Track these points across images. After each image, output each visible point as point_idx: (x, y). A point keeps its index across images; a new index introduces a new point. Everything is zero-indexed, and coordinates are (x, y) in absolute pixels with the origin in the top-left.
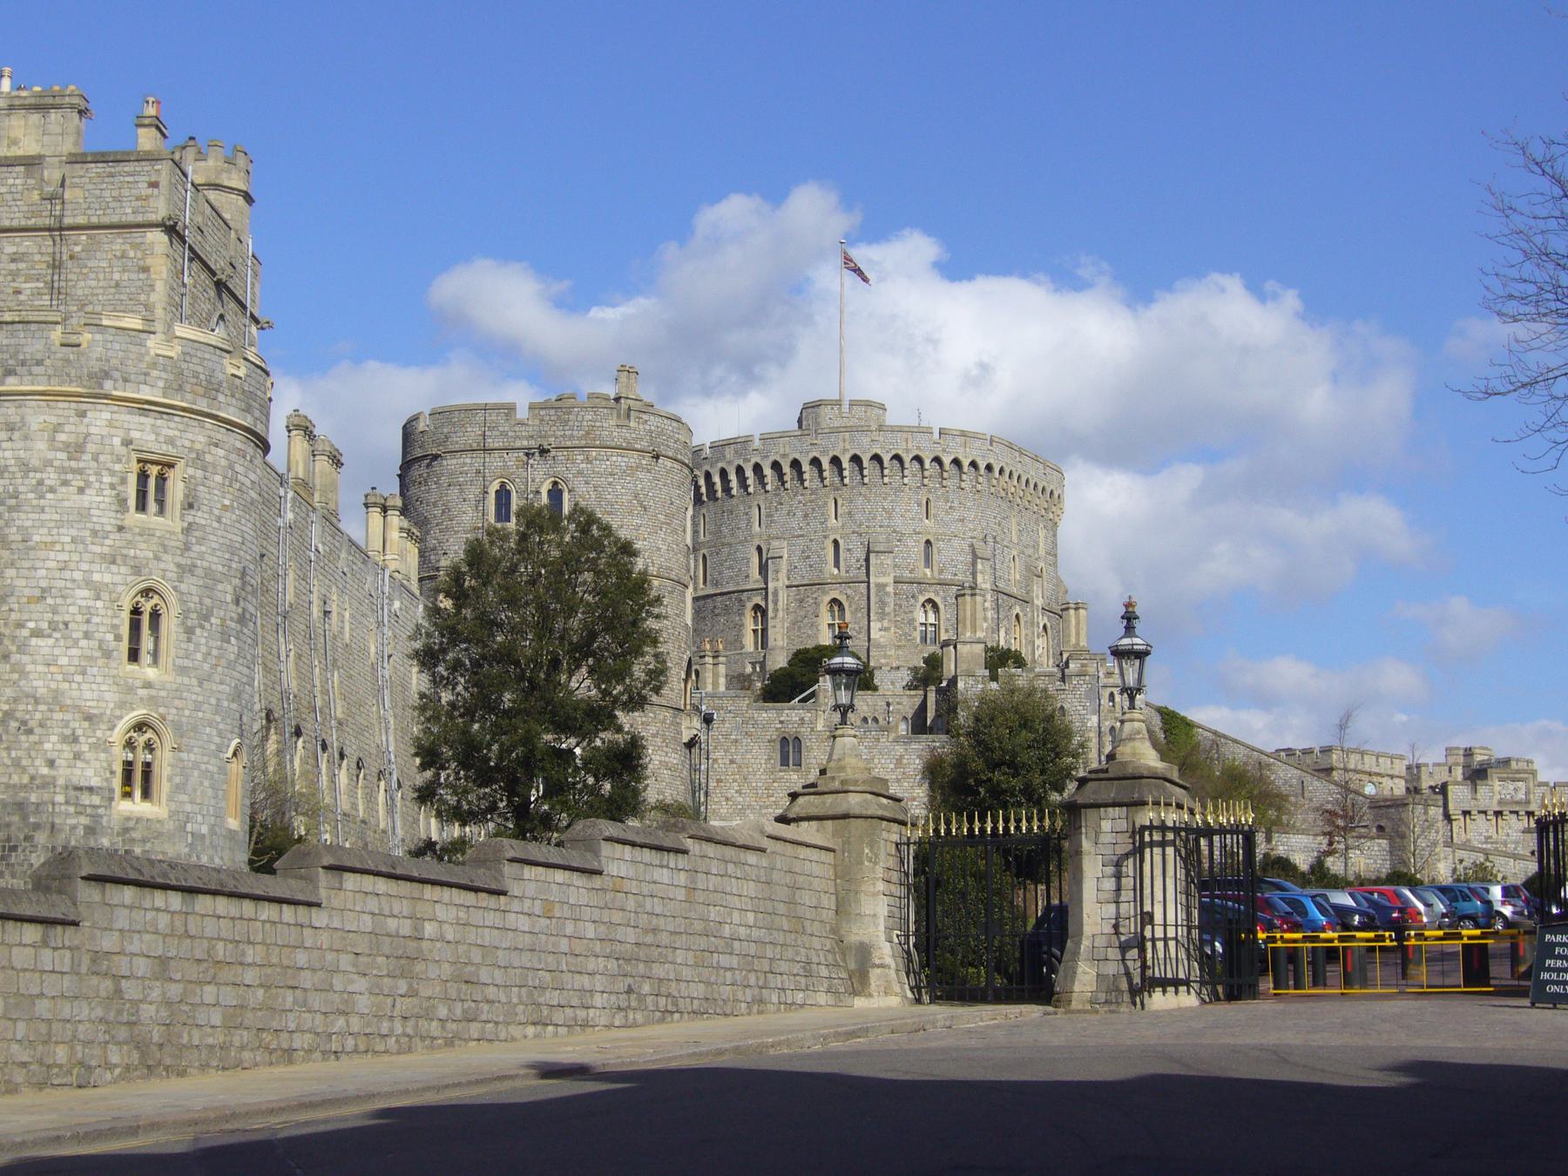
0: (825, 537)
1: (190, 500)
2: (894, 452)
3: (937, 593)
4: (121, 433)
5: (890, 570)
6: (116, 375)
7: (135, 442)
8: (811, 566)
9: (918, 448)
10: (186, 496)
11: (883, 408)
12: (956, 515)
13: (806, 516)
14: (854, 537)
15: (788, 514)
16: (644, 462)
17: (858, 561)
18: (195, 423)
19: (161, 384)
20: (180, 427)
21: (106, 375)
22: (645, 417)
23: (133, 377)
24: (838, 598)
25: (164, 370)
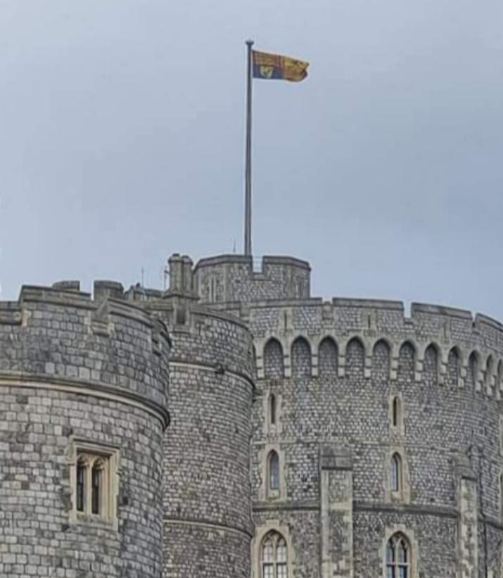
0: (260, 447)
1: (125, 494)
2: (352, 335)
3: (409, 526)
4: (62, 421)
6: (57, 356)
7: (76, 431)
9: (385, 330)
10: (121, 490)
11: (306, 267)
12: (433, 421)
16: (206, 379)
18: (125, 409)
19: (99, 366)
20: (115, 413)
21: (47, 356)
22: (207, 321)
23: (73, 358)
24: (278, 528)
25: (101, 351)
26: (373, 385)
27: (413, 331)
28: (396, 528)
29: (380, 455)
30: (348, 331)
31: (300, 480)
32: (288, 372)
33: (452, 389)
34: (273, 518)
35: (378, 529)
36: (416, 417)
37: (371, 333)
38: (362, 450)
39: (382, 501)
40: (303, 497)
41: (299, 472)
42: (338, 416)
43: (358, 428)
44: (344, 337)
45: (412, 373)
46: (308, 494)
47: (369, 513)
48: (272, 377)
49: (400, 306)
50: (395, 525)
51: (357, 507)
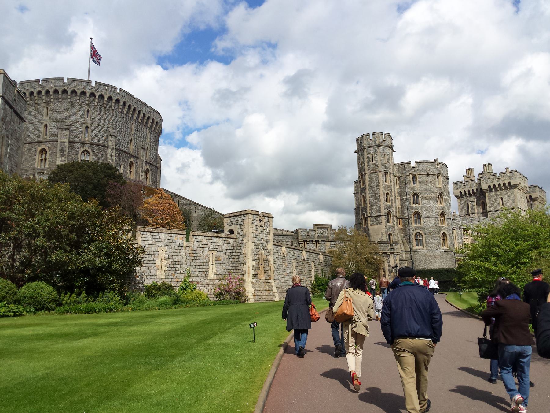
0: (42, 123)
2: (73, 89)
3: (89, 148)
5: (68, 137)
9: (84, 88)
13: (35, 115)
14: (54, 123)
28: (85, 148)
35: (78, 148)
37: (79, 89)
49: (90, 82)
51: (70, 142)
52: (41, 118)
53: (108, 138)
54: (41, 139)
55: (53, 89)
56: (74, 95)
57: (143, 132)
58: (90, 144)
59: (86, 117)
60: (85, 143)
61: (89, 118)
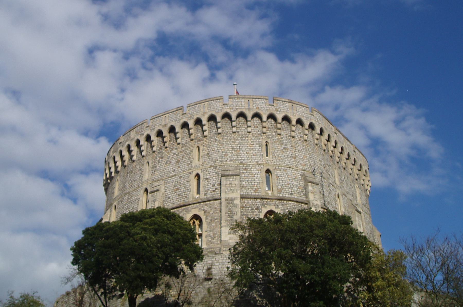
0: (190, 173)
2: (239, 111)
8: (179, 195)
9: (258, 108)
12: (289, 153)
13: (178, 162)
14: (211, 170)
15: (166, 163)
17: (213, 186)
26: (253, 136)
27: (274, 109)
28: (269, 208)
29: (257, 170)
30: (237, 109)
31: (211, 186)
32: (206, 133)
33: (300, 140)
34: (195, 208)
35: (257, 209)
36: (279, 152)
38: (247, 168)
39: (260, 194)
40: (213, 195)
41: (210, 182)
42: (233, 151)
43: (244, 156)
44: (235, 112)
45: (275, 130)
46: (215, 193)
47: (252, 200)
48: (198, 138)
50: (268, 206)
51: (242, 198)
52: (189, 164)
53: (305, 189)
54: (190, 200)
55: (207, 116)
56: (241, 119)
57: (351, 185)
58: (279, 199)
59: (265, 155)
60: (269, 199)
61: (270, 156)
